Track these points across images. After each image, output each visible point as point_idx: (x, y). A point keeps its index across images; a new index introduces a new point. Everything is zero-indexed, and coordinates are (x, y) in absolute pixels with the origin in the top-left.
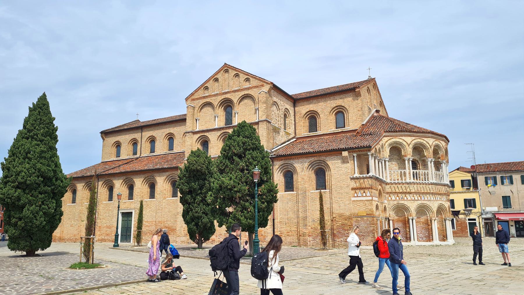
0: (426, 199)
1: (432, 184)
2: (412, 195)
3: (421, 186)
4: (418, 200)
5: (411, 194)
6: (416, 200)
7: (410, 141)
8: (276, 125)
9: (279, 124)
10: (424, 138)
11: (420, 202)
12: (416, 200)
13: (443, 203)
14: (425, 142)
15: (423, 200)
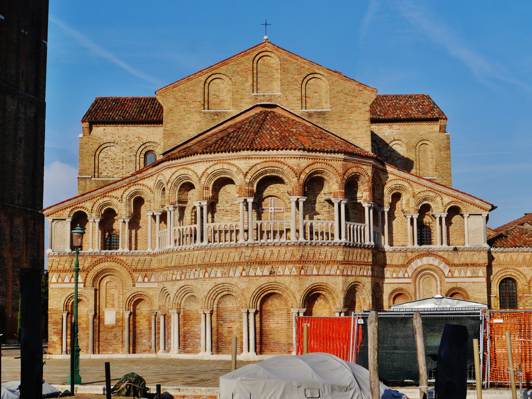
0: (192, 277)
1: (199, 249)
2: (172, 272)
3: (183, 254)
4: (181, 279)
5: (170, 270)
6: (178, 280)
7: (169, 177)
8: (114, 176)
9: (124, 173)
10: (189, 166)
11: (182, 283)
12: (178, 280)
13: (234, 281)
14: (190, 173)
15: (187, 279)
